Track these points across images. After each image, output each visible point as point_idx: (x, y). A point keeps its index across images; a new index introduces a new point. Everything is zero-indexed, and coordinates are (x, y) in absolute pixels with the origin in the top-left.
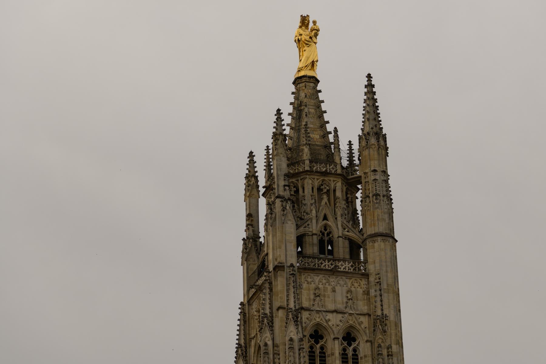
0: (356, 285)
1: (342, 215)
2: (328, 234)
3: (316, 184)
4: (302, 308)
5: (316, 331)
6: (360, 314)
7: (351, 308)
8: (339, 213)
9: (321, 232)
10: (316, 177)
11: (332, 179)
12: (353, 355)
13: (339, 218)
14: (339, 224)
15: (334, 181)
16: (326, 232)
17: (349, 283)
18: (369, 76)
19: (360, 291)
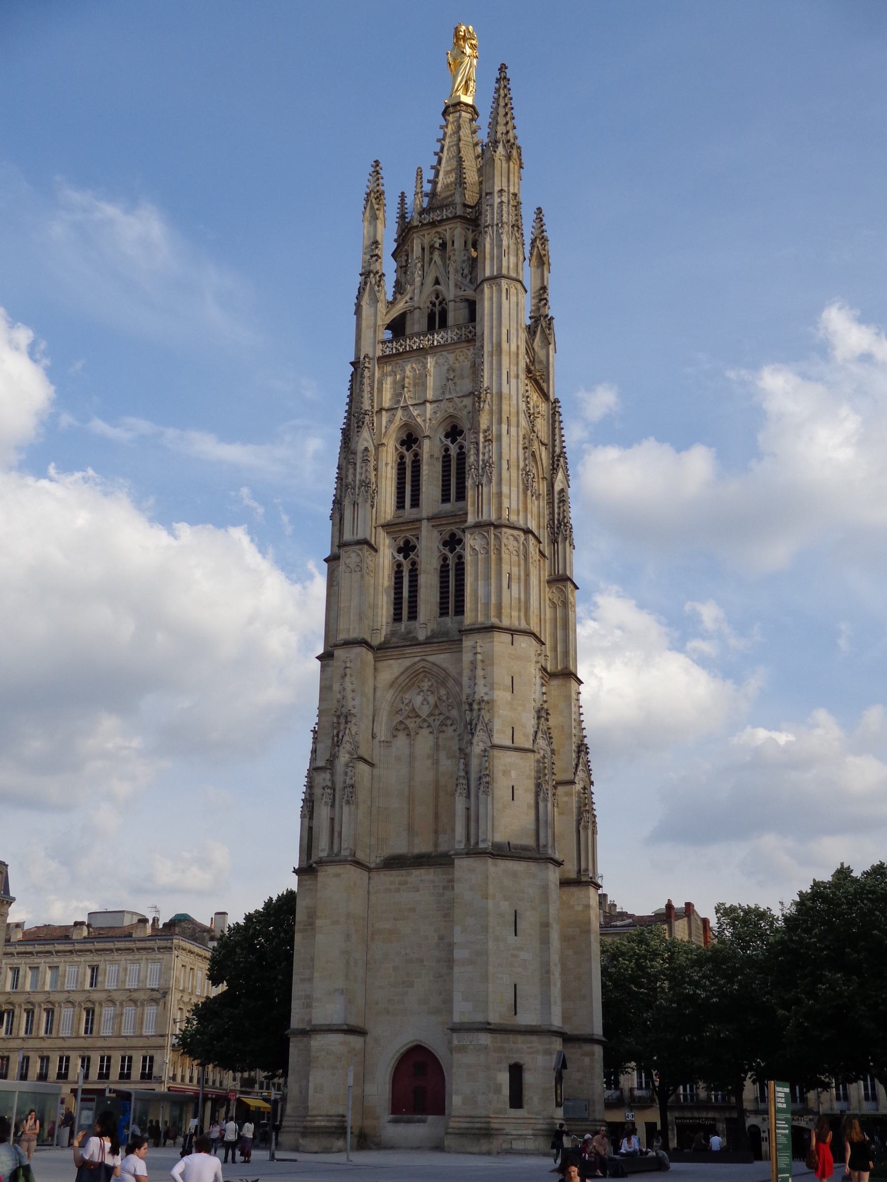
0: (461, 359)
1: (456, 271)
2: (441, 303)
3: (426, 240)
4: (381, 409)
5: (410, 435)
6: (463, 396)
7: (450, 392)
8: (451, 270)
9: (431, 303)
10: (426, 232)
11: (447, 227)
12: (458, 454)
13: (451, 276)
14: (452, 283)
15: (450, 229)
16: (437, 302)
17: (451, 357)
18: (503, 68)
19: (467, 364)
